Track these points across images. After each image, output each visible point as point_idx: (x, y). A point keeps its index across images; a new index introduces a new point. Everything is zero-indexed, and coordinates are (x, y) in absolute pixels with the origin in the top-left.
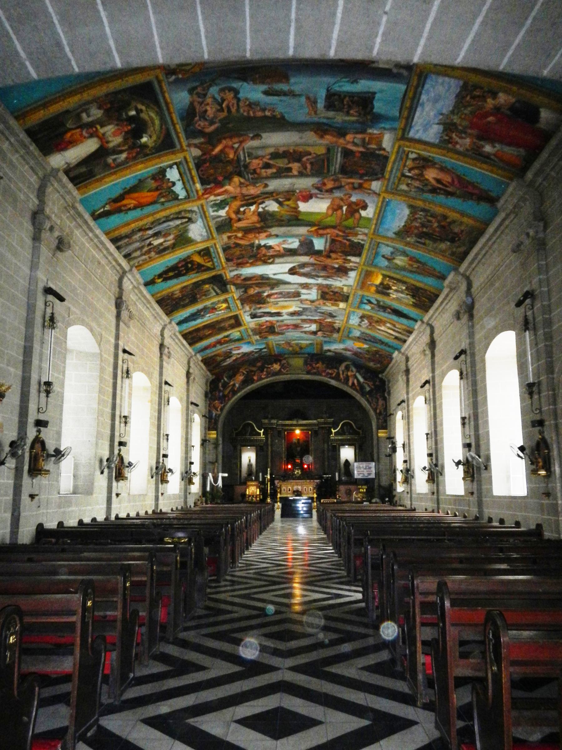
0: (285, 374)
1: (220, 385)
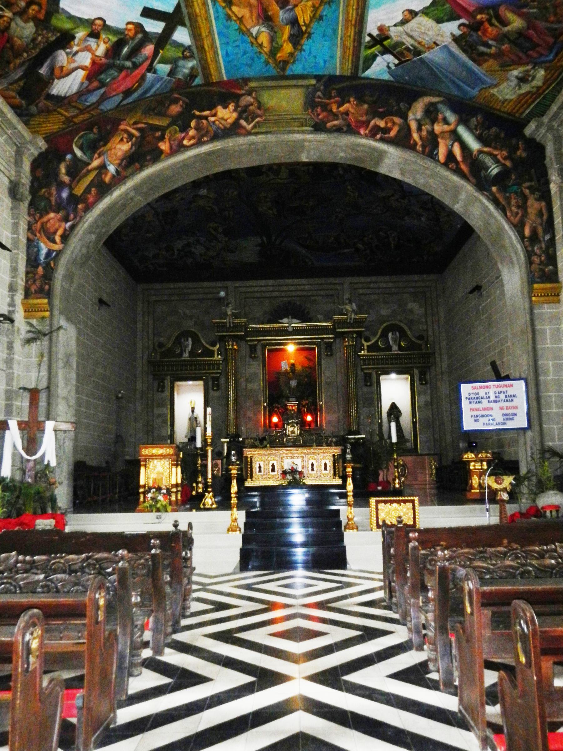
0: (249, 133)
1: (63, 169)
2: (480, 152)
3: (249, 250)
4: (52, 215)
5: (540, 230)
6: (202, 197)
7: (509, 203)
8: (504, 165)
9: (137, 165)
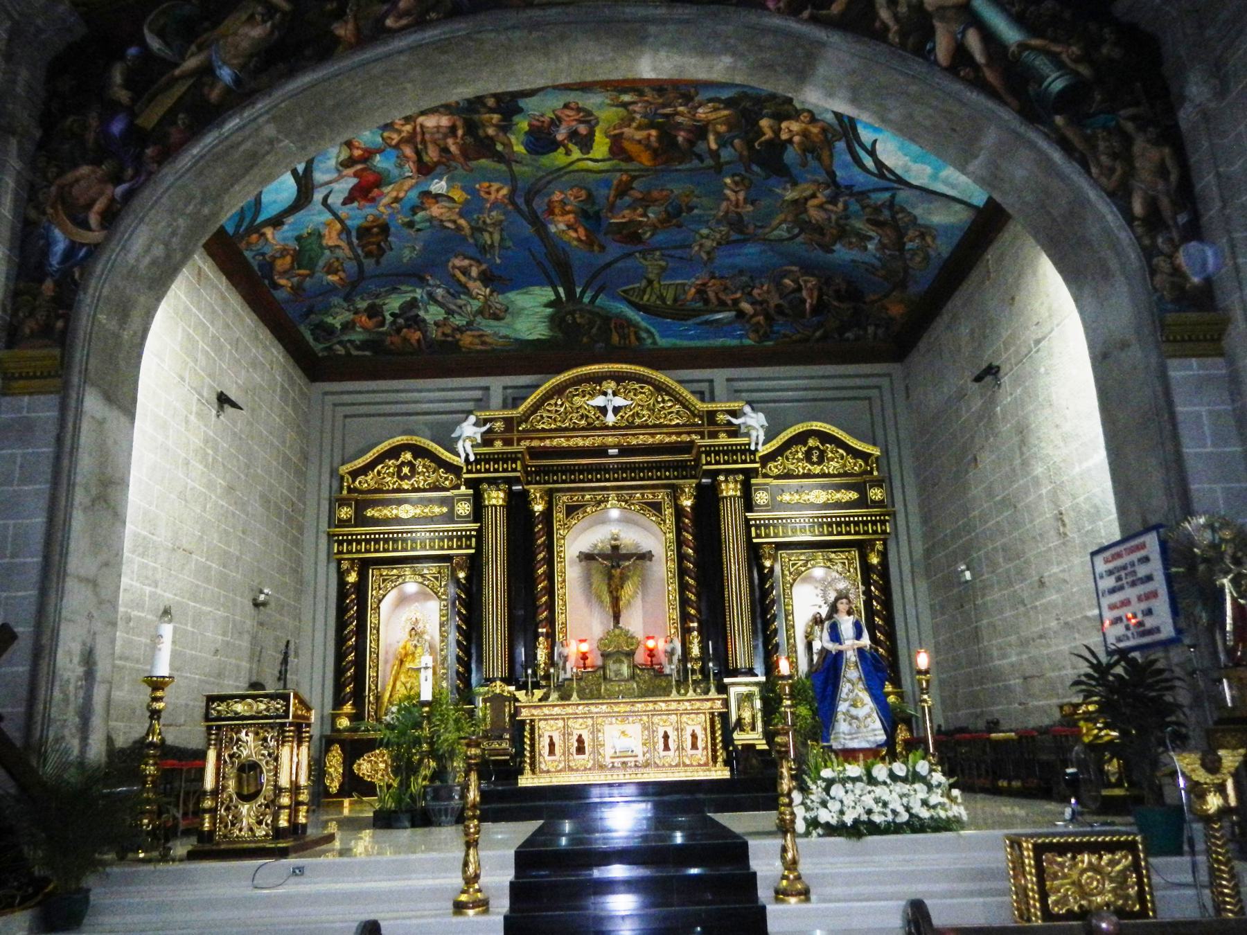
1: (118, 78)
2: (1023, 46)
3: (530, 314)
4: (85, 170)
5: (1165, 203)
6: (437, 197)
7: (1094, 148)
8: (1077, 73)
9: (281, 66)
